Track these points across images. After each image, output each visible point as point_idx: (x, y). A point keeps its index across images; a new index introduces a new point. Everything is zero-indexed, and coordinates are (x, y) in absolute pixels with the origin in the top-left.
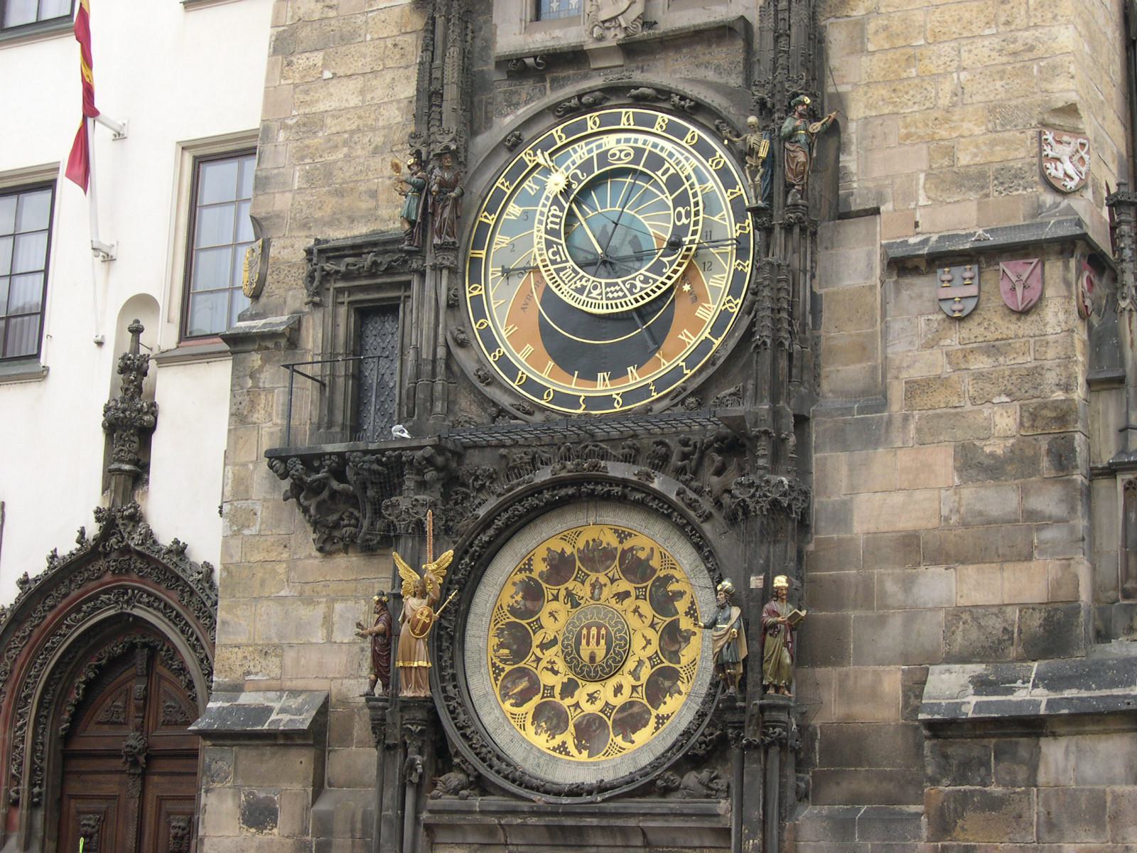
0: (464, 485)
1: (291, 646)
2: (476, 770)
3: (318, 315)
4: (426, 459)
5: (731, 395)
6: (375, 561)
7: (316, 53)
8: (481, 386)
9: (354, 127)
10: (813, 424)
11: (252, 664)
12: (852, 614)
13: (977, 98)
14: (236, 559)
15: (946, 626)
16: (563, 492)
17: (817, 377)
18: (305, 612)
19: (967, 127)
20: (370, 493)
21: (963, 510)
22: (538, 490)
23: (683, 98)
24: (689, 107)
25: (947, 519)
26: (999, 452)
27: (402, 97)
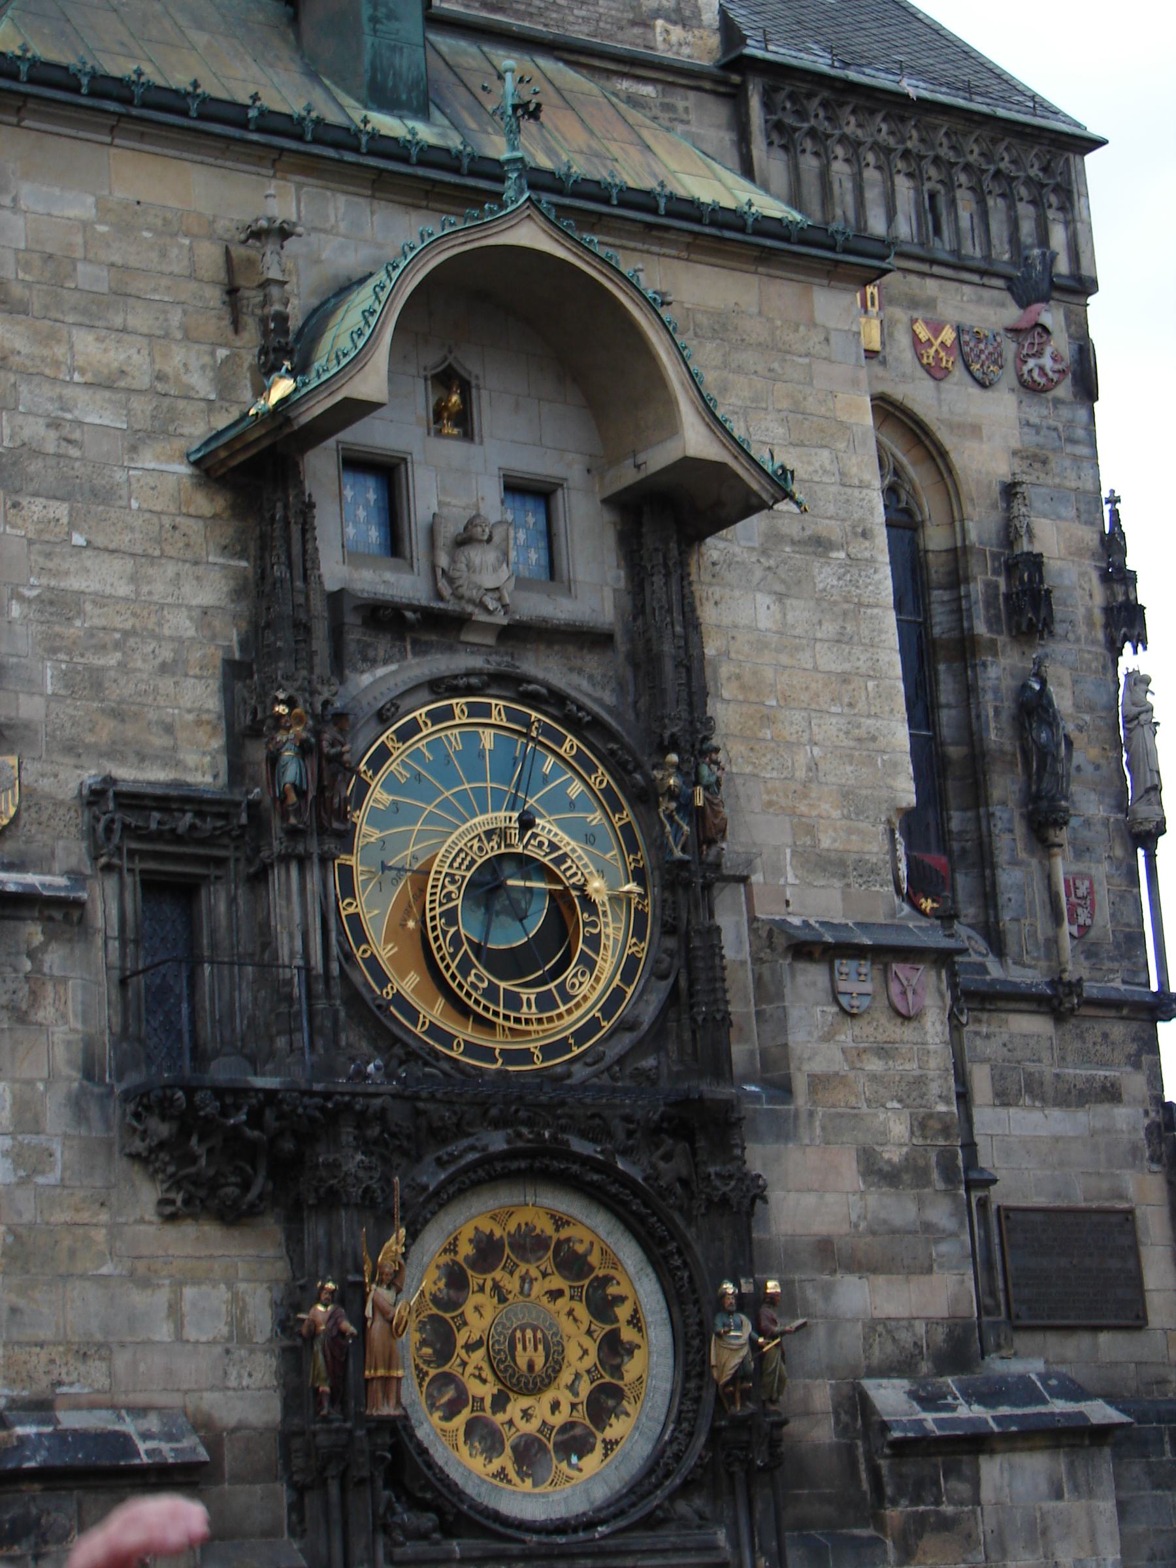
1: (122, 1345)
2: (454, 1506)
3: (111, 883)
5: (657, 1068)
6: (237, 1233)
7: (54, 504)
9: (128, 625)
11: (64, 1370)
13: (831, 779)
14: (27, 1217)
16: (514, 1165)
18: (139, 1298)
19: (825, 807)
22: (489, 1159)
23: (580, 708)
25: (856, 1226)
26: (896, 1159)
27: (194, 603)
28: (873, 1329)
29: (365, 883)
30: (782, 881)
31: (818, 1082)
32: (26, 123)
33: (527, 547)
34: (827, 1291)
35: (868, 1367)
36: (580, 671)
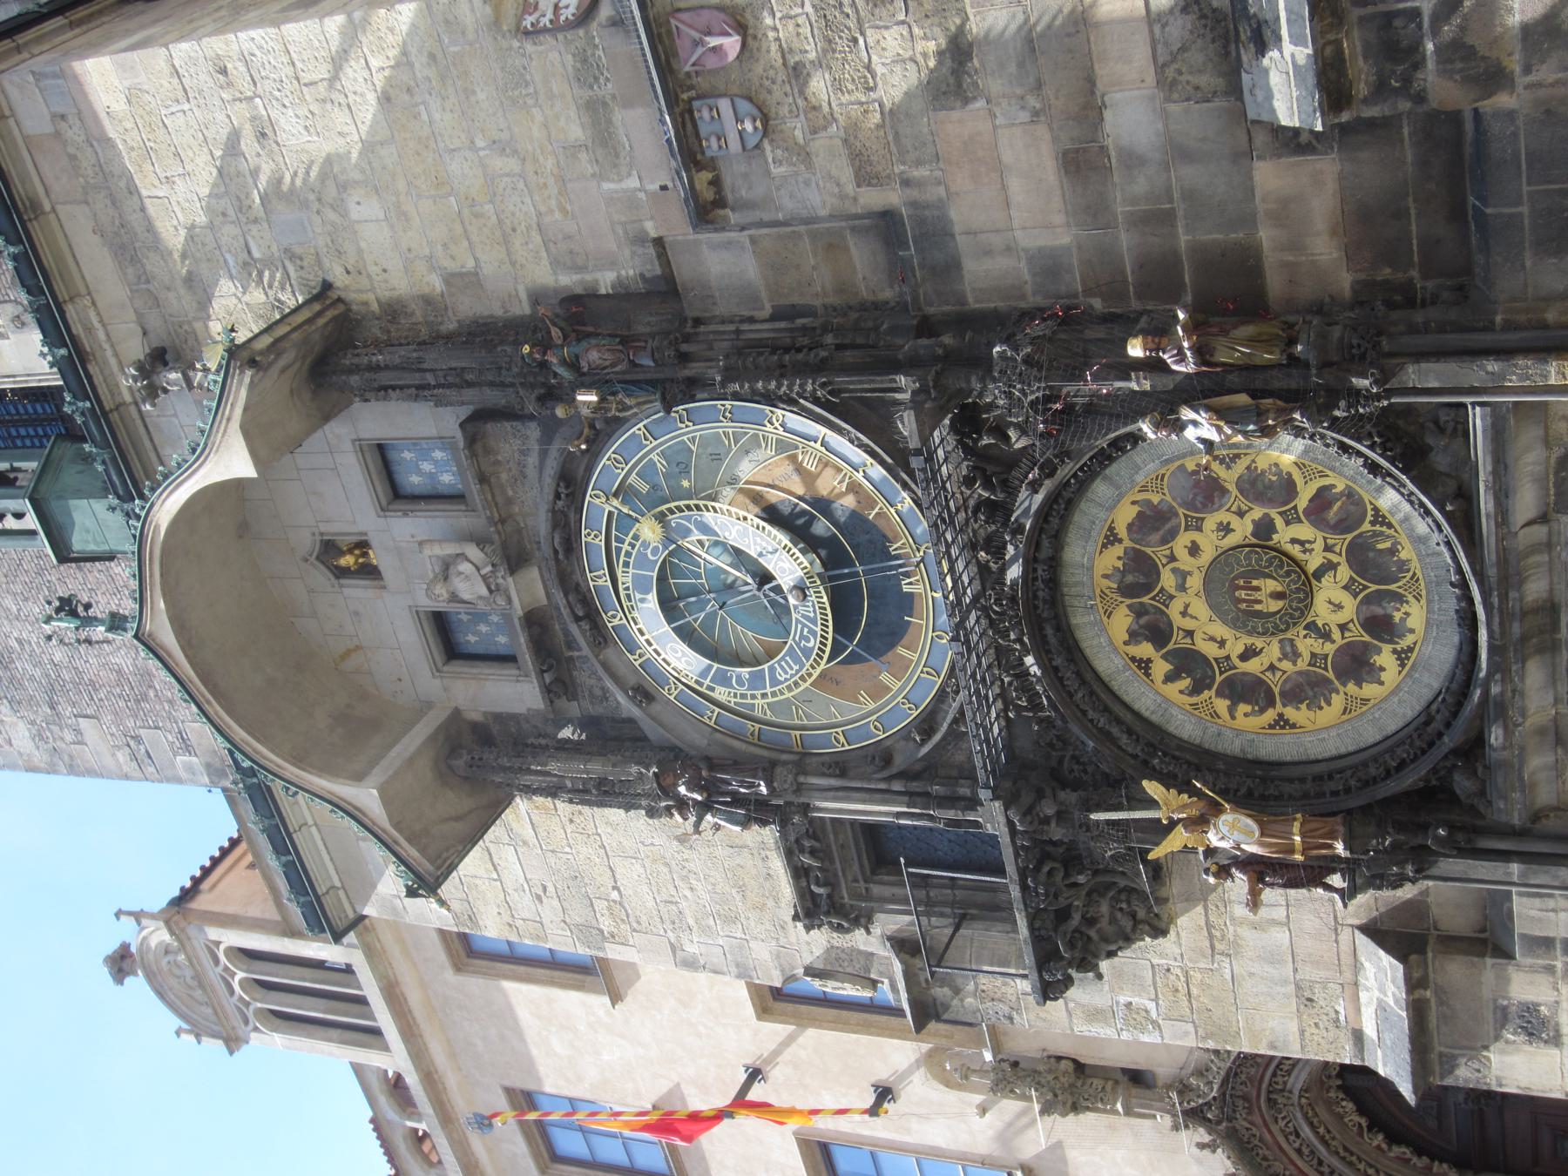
0: (1061, 762)
1: (1295, 970)
2: (1446, 757)
4: (1024, 815)
8: (937, 737)
9: (666, 870)
10: (931, 310)
12: (1183, 239)
14: (1190, 1027)
15: (1188, 100)
17: (877, 306)
19: (537, 132)
20: (1081, 879)
21: (1019, 91)
23: (558, 496)
24: (567, 487)
25: (1036, 113)
28: (1174, 83)
29: (808, 717)
30: (642, 195)
31: (866, 175)
32: (338, 884)
33: (436, 462)
34: (1133, 160)
35: (1227, 93)
36: (522, 465)
